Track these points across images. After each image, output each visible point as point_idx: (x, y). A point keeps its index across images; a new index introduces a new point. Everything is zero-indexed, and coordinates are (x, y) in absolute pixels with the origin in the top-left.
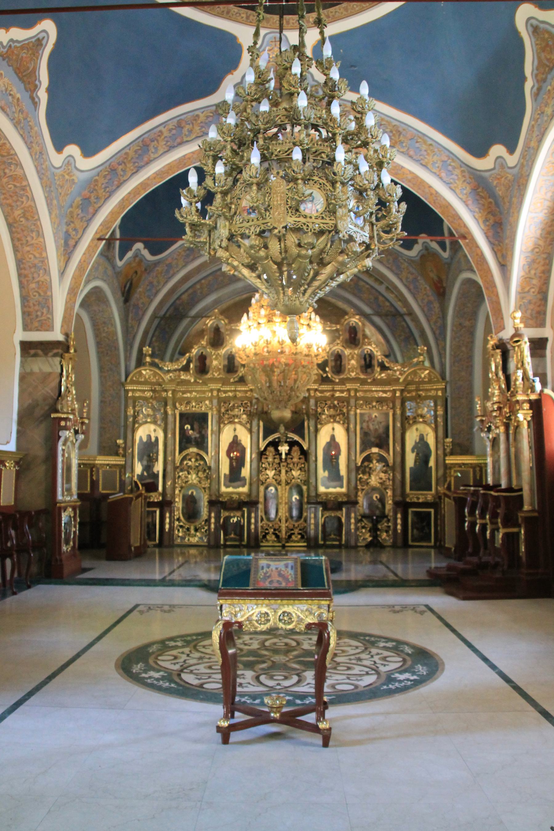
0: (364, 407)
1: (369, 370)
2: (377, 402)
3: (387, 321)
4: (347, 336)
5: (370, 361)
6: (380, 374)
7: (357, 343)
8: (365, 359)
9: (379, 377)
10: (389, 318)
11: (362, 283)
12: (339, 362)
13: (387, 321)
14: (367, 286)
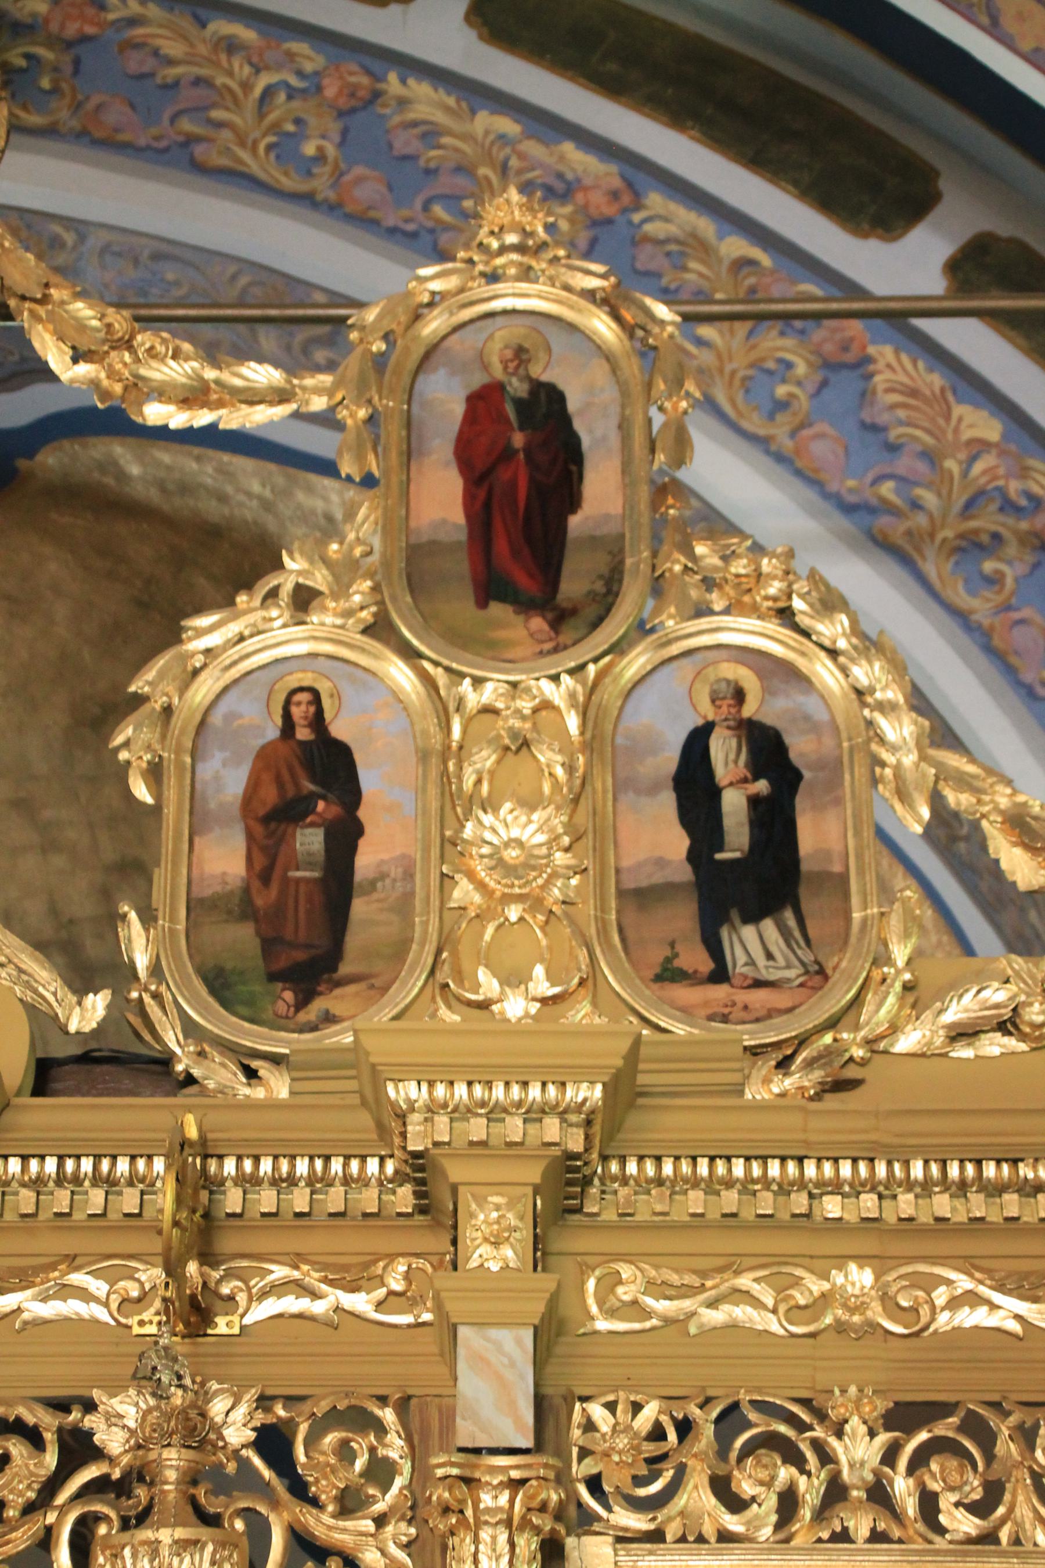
0: (697, 1497)
1: (751, 943)
2: (903, 1417)
3: (981, 606)
4: (441, 499)
5: (774, 819)
6: (916, 997)
7: (573, 585)
8: (694, 785)
9: (907, 1042)
10: (1009, 567)
11: (665, 217)
12: (310, 840)
13: (981, 606)
14: (735, 246)
